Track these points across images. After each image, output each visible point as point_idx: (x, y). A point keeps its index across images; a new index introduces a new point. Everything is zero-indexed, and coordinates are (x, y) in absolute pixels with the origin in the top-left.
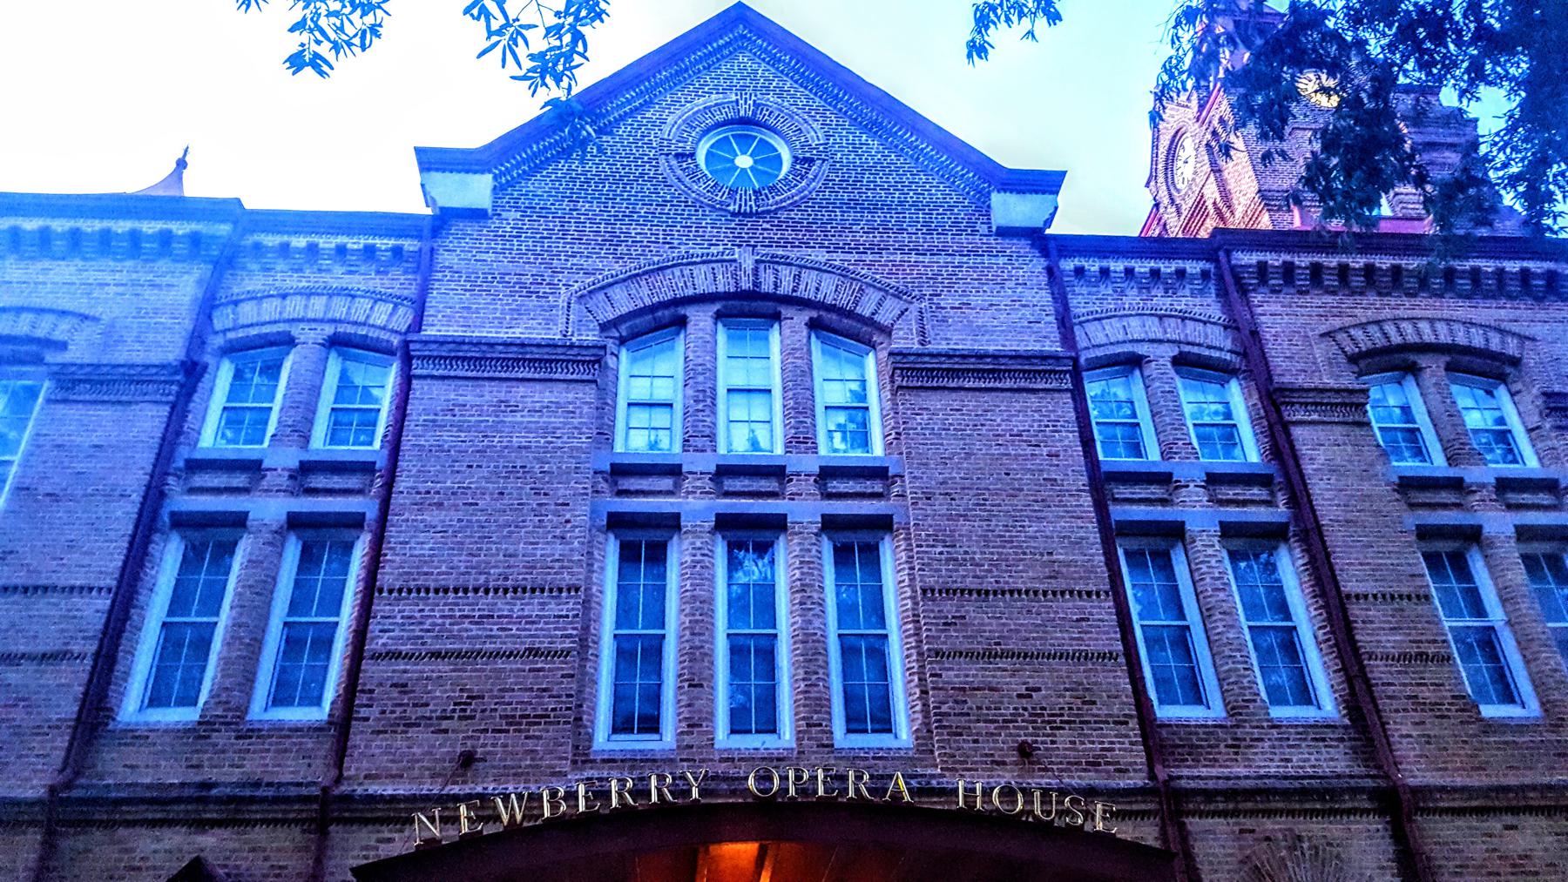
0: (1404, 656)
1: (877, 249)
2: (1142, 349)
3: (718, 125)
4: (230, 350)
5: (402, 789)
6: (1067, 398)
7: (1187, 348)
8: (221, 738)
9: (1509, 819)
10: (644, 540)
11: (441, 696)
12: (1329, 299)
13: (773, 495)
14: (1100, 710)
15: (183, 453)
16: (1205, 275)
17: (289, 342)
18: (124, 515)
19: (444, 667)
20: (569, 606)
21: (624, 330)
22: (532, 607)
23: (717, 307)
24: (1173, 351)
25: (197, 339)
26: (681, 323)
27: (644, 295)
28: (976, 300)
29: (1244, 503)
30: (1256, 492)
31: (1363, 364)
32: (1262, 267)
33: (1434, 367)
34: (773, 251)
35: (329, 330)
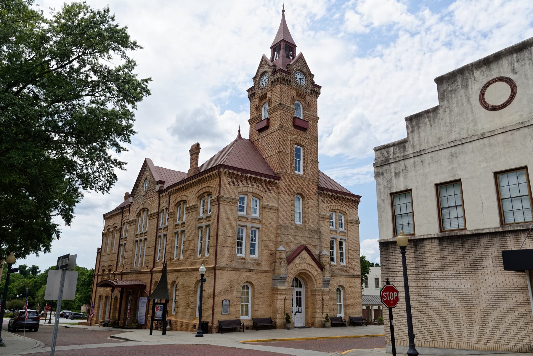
1: (150, 198)
18: (118, 245)
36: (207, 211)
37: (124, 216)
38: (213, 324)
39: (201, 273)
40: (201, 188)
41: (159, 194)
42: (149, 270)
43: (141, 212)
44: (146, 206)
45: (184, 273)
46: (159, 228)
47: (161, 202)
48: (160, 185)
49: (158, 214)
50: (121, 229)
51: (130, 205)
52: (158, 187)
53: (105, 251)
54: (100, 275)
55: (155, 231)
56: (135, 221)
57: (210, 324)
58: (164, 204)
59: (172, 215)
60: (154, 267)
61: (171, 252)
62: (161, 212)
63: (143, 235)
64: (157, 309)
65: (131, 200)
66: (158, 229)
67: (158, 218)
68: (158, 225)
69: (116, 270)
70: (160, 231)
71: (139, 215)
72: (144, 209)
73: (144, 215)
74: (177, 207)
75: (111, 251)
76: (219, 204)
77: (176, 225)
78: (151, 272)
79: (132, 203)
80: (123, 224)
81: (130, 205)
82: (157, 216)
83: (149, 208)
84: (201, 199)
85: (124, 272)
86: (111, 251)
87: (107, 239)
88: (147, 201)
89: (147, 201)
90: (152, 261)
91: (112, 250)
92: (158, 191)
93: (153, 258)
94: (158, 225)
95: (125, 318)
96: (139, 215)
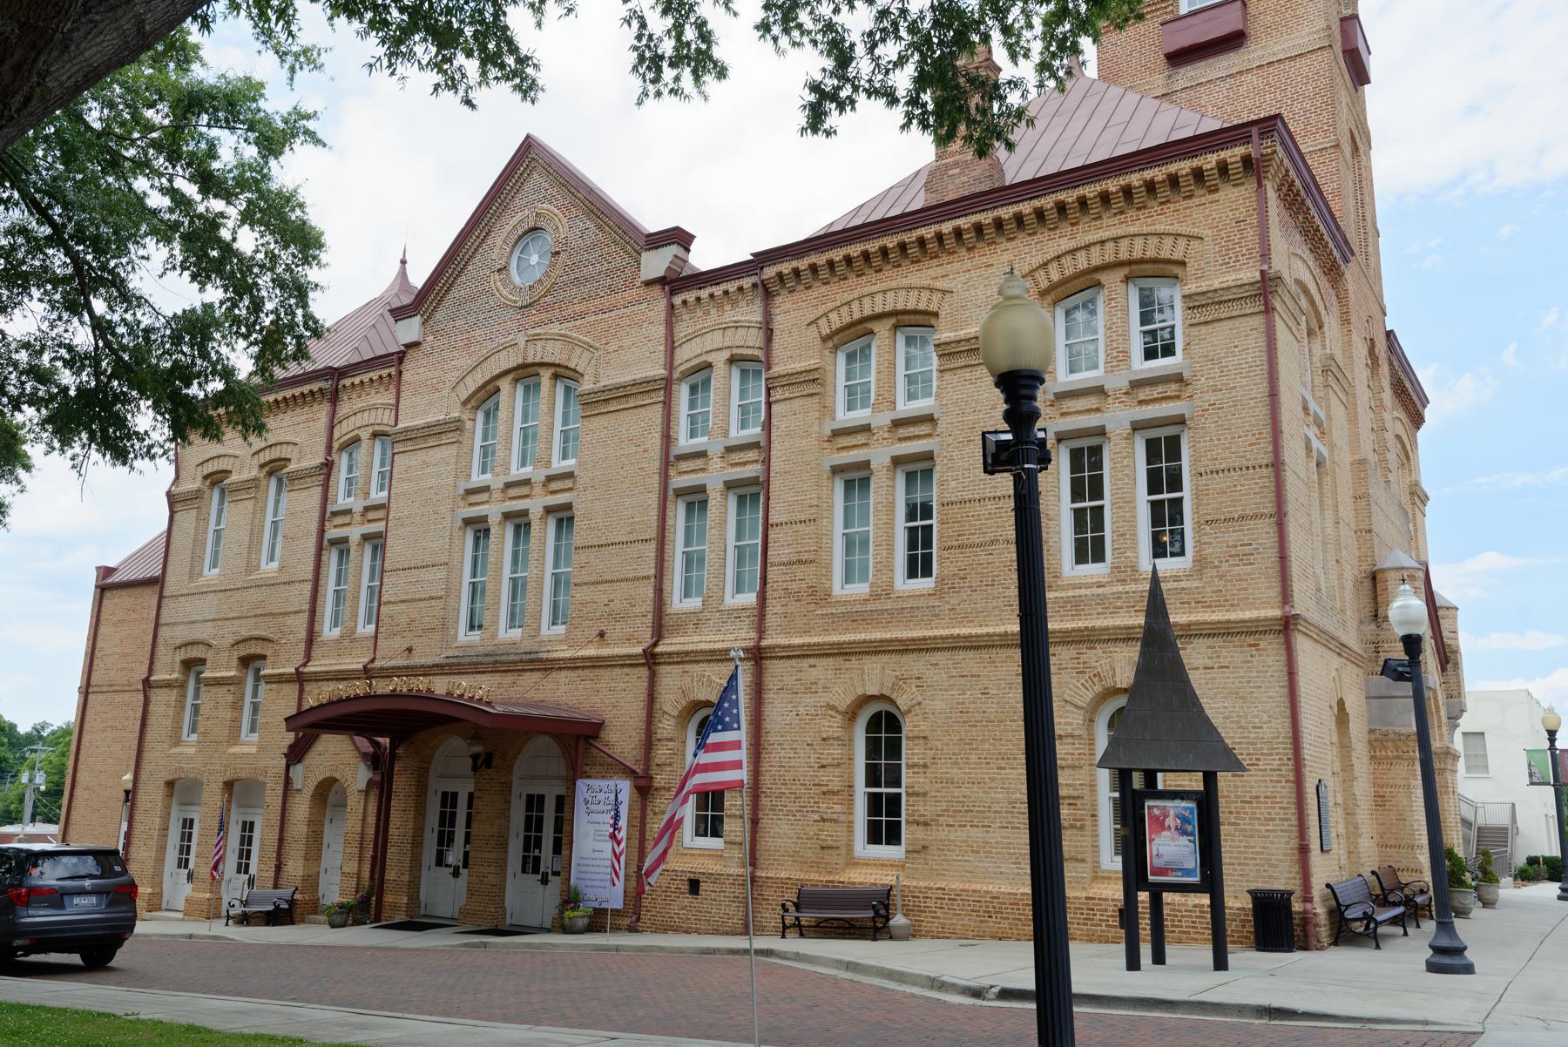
0: (791, 563)
2: (709, 358)
3: (520, 237)
4: (342, 449)
5: (393, 663)
6: (659, 408)
7: (736, 351)
8: (346, 643)
9: (812, 661)
10: (479, 528)
11: (403, 620)
12: (823, 289)
13: (527, 496)
14: (637, 610)
15: (330, 508)
16: (755, 286)
17: (357, 440)
18: (312, 543)
19: (403, 606)
20: (441, 574)
21: (473, 403)
22: (423, 575)
23: (512, 376)
24: (726, 354)
25: (329, 448)
26: (498, 390)
27: (479, 378)
28: (626, 342)
29: (745, 464)
30: (752, 455)
31: (836, 339)
32: (780, 275)
33: (882, 329)
34: (538, 331)
35: (370, 430)
36: (1126, 356)
37: (344, 409)
38: (1307, 899)
39: (1401, 631)
40: (1065, 244)
41: (672, 293)
42: (639, 650)
43: (505, 384)
44: (553, 352)
45: (972, 654)
46: (675, 451)
47: (682, 330)
48: (673, 250)
49: (667, 384)
50: (328, 466)
51: (400, 357)
52: (656, 263)
53: (195, 573)
54: (168, 685)
55: (655, 465)
56: (456, 426)
57: (1297, 906)
58: (715, 339)
59: (811, 381)
60: (659, 632)
61: (811, 560)
62: (680, 380)
63: (538, 489)
64: (1160, 824)
65: (410, 330)
66: (669, 460)
67: (668, 405)
68: (667, 438)
69: (308, 657)
70: (684, 466)
71: (485, 398)
72: (525, 373)
73: (511, 398)
74: (836, 348)
75: (248, 571)
76: (1268, 310)
77: (837, 433)
78: (651, 659)
79: (415, 345)
80: (338, 446)
81: (400, 357)
82: (660, 396)
83: (579, 361)
84: (1055, 303)
85: (377, 664)
86: (248, 571)
87: (202, 520)
88: (555, 328)
89: (555, 328)
90: (648, 606)
91: (251, 566)
92: (648, 283)
93: (648, 591)
94: (667, 438)
95: (414, 886)
96: (485, 398)
